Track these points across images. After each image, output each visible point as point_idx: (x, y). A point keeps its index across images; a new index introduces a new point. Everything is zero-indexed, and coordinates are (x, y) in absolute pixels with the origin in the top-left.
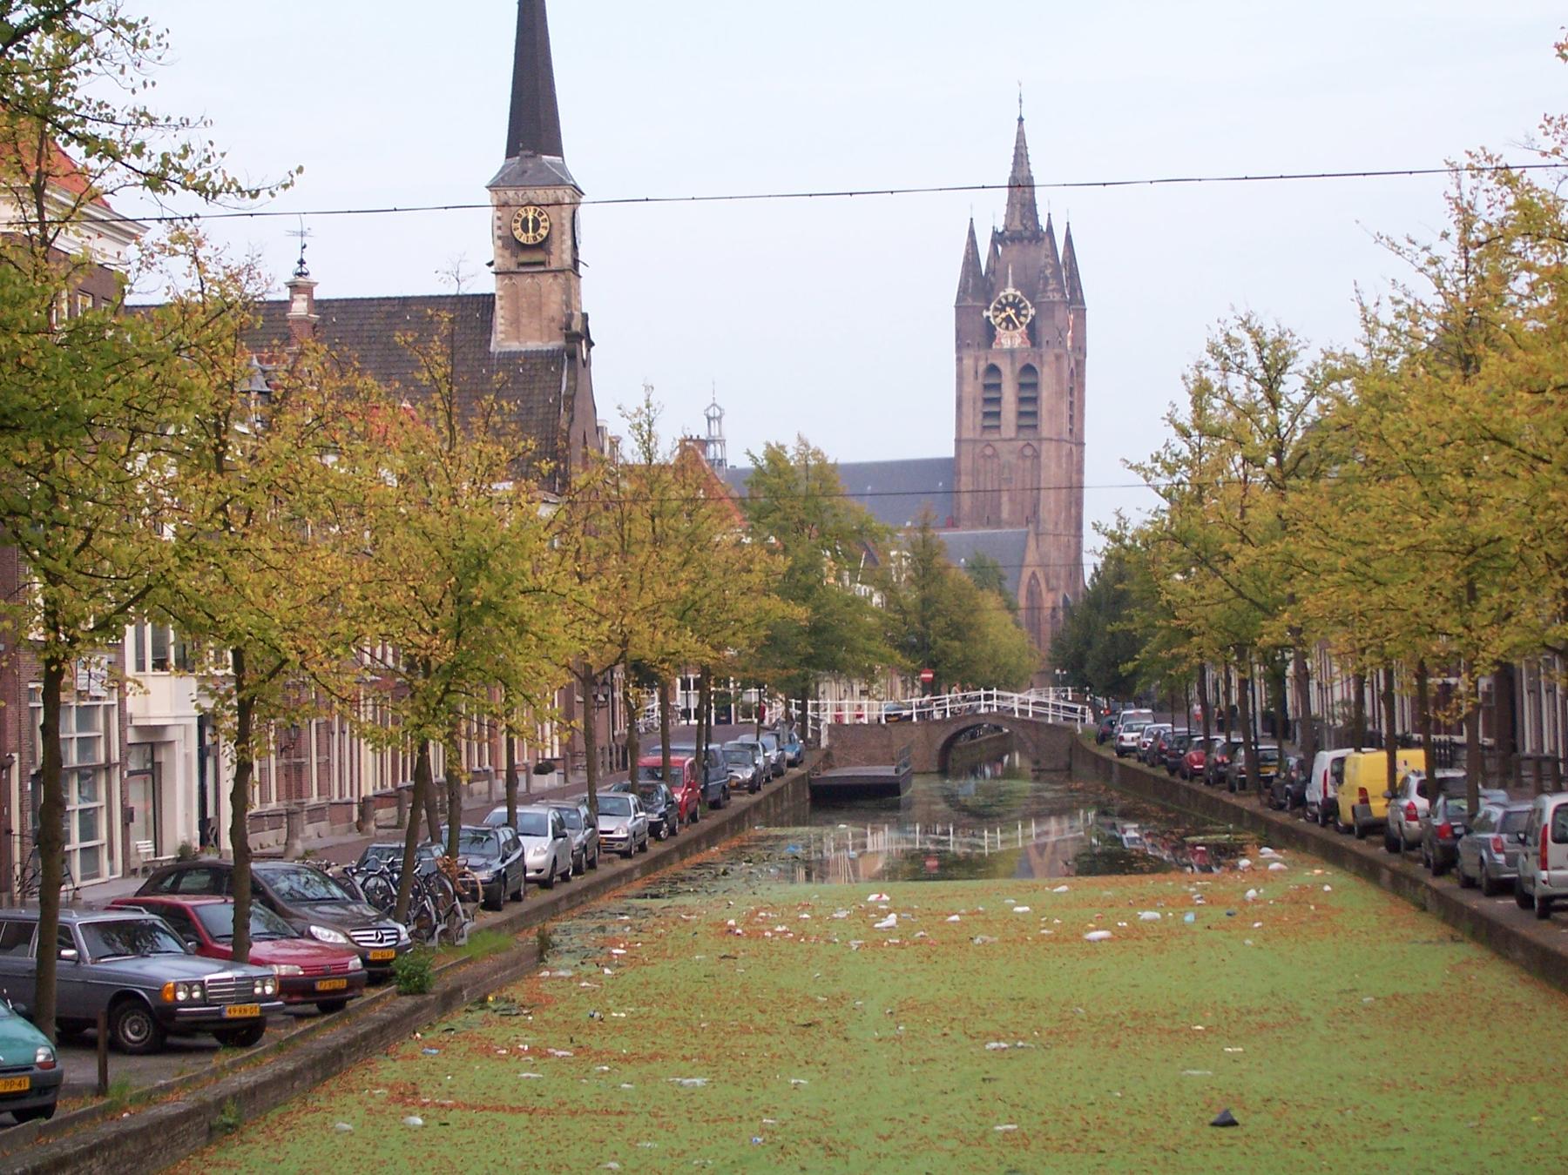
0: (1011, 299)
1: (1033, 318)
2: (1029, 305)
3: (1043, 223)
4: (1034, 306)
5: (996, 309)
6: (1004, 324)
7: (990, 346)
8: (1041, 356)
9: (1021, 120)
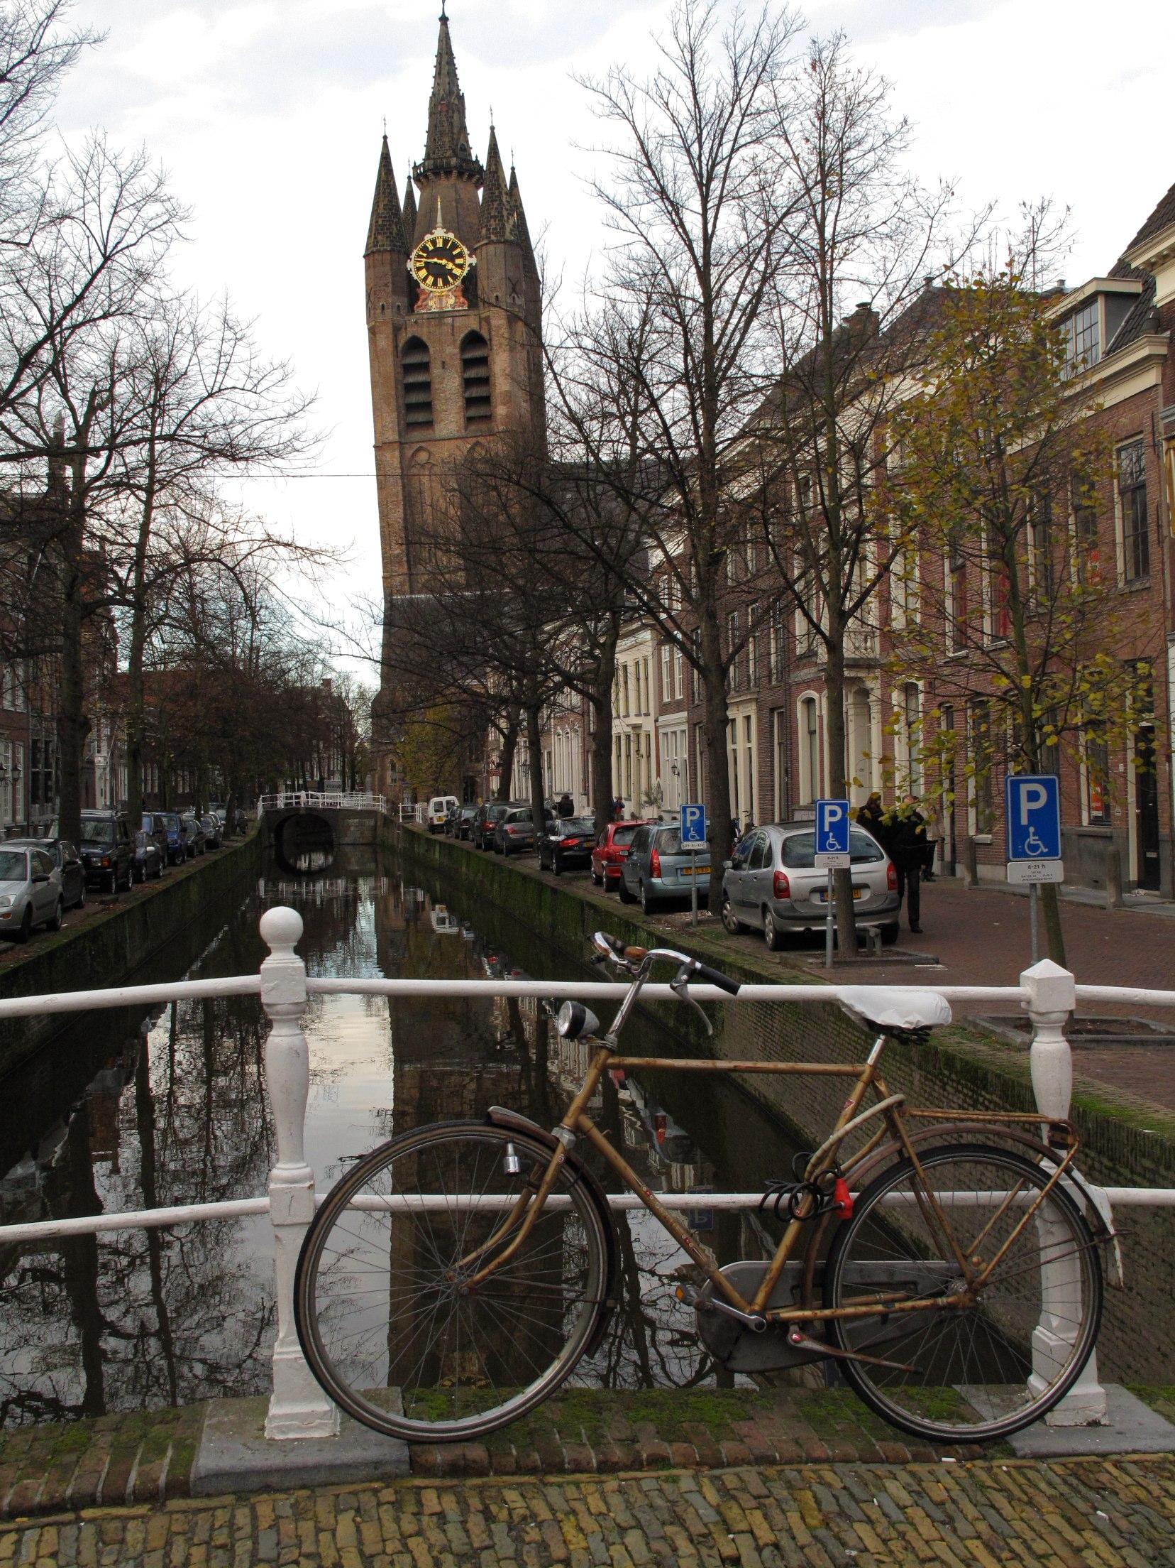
0: (440, 244)
2: (466, 252)
3: (479, 152)
4: (473, 252)
6: (431, 280)
7: (413, 311)
8: (487, 320)
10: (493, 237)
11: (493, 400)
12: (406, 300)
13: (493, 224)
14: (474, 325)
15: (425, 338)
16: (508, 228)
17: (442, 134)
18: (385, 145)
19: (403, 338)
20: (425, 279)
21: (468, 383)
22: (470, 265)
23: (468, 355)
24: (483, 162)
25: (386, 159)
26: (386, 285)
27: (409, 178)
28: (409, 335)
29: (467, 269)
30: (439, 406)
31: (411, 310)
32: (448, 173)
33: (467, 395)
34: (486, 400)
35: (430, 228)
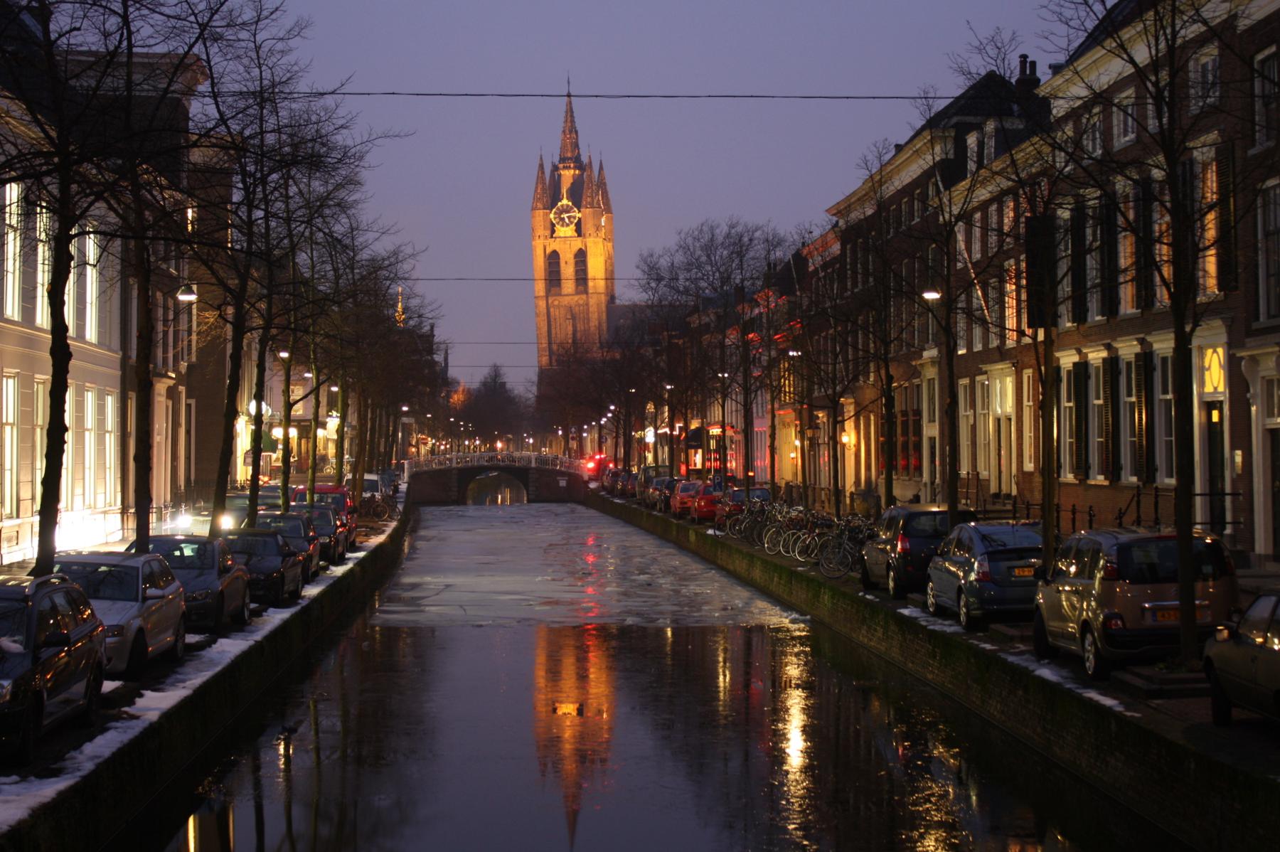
1: (580, 219)
3: (585, 159)
16: (595, 201)
18: (541, 159)
19: (548, 251)
25: (541, 166)
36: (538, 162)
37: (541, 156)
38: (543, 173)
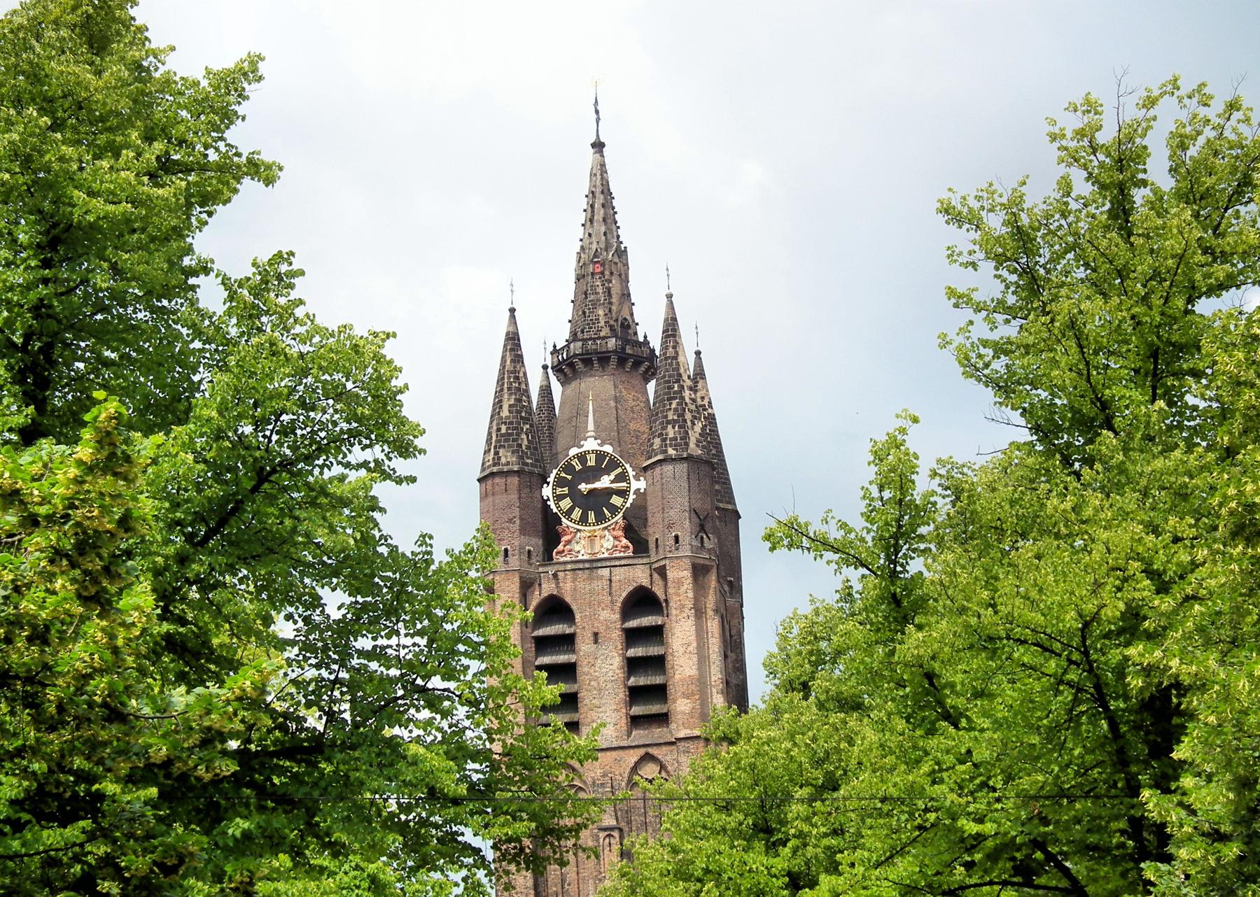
0: (591, 462)
3: (649, 328)
5: (560, 482)
6: (577, 513)
7: (551, 558)
8: (662, 572)
9: (598, 146)
10: (671, 452)
11: (671, 690)
12: (540, 542)
13: (671, 432)
14: (640, 575)
15: (568, 599)
16: (694, 436)
17: (595, 304)
20: (568, 513)
21: (633, 665)
22: (637, 491)
23: (633, 623)
24: (656, 343)
25: (513, 340)
26: (510, 521)
27: (545, 367)
28: (545, 594)
29: (632, 497)
30: (586, 699)
31: (548, 557)
32: (604, 359)
33: (632, 681)
34: (660, 692)
35: (576, 440)
36: (503, 328)
37: (512, 311)
38: (518, 359)
